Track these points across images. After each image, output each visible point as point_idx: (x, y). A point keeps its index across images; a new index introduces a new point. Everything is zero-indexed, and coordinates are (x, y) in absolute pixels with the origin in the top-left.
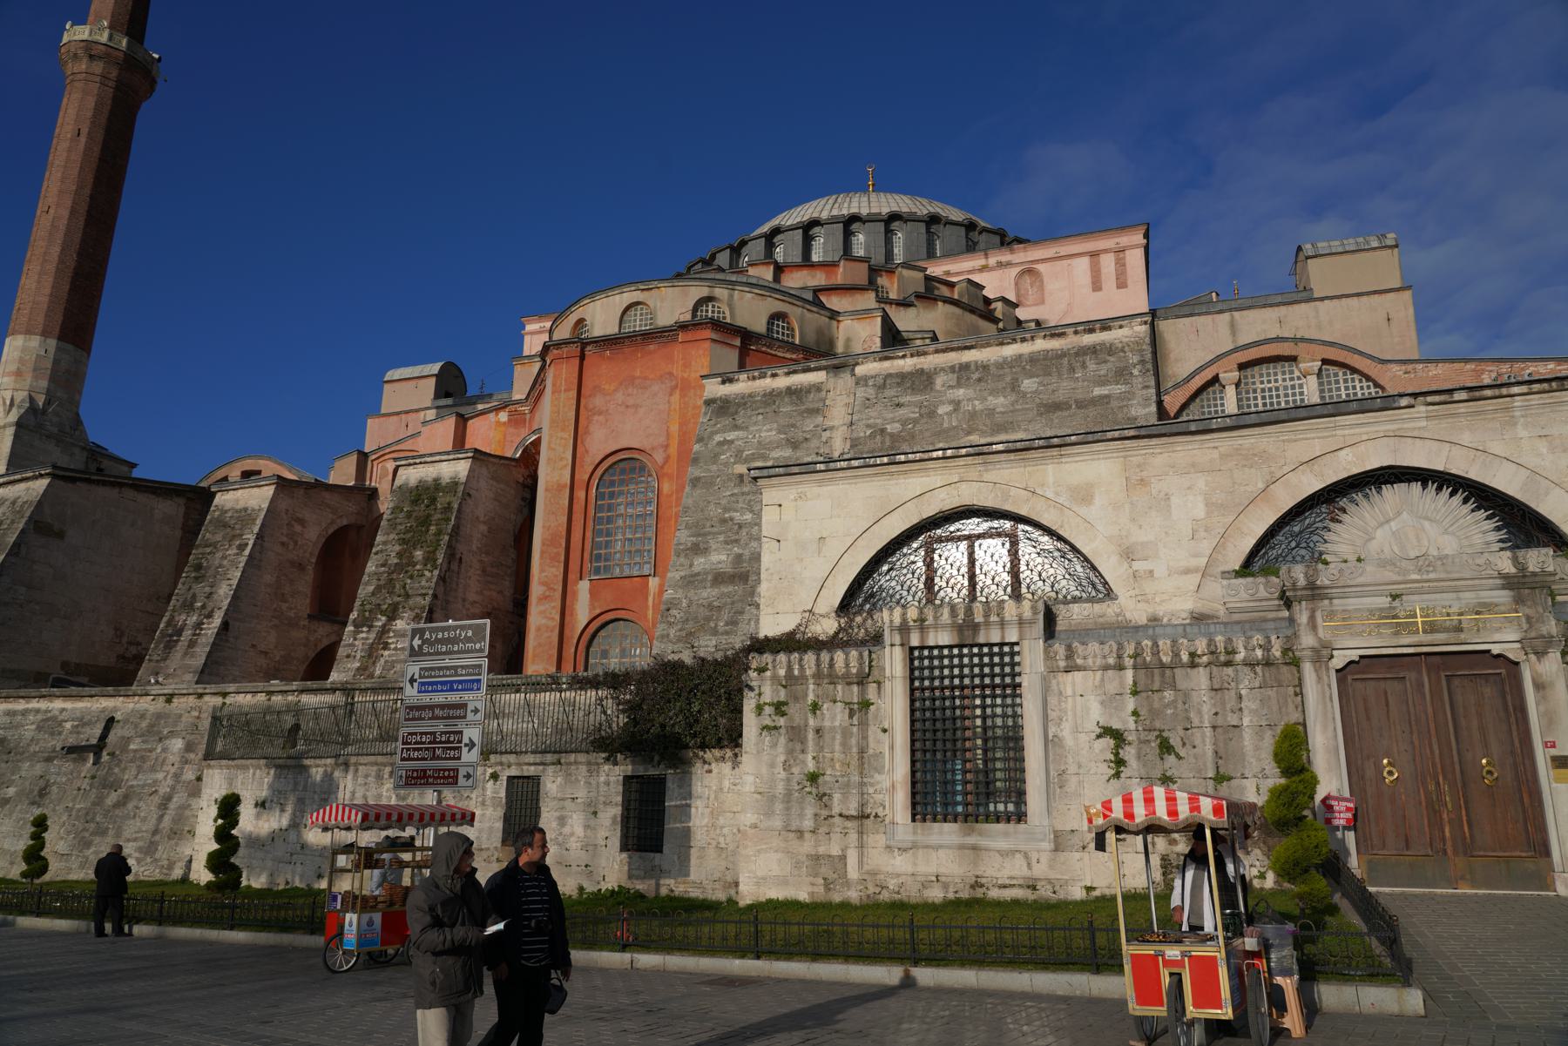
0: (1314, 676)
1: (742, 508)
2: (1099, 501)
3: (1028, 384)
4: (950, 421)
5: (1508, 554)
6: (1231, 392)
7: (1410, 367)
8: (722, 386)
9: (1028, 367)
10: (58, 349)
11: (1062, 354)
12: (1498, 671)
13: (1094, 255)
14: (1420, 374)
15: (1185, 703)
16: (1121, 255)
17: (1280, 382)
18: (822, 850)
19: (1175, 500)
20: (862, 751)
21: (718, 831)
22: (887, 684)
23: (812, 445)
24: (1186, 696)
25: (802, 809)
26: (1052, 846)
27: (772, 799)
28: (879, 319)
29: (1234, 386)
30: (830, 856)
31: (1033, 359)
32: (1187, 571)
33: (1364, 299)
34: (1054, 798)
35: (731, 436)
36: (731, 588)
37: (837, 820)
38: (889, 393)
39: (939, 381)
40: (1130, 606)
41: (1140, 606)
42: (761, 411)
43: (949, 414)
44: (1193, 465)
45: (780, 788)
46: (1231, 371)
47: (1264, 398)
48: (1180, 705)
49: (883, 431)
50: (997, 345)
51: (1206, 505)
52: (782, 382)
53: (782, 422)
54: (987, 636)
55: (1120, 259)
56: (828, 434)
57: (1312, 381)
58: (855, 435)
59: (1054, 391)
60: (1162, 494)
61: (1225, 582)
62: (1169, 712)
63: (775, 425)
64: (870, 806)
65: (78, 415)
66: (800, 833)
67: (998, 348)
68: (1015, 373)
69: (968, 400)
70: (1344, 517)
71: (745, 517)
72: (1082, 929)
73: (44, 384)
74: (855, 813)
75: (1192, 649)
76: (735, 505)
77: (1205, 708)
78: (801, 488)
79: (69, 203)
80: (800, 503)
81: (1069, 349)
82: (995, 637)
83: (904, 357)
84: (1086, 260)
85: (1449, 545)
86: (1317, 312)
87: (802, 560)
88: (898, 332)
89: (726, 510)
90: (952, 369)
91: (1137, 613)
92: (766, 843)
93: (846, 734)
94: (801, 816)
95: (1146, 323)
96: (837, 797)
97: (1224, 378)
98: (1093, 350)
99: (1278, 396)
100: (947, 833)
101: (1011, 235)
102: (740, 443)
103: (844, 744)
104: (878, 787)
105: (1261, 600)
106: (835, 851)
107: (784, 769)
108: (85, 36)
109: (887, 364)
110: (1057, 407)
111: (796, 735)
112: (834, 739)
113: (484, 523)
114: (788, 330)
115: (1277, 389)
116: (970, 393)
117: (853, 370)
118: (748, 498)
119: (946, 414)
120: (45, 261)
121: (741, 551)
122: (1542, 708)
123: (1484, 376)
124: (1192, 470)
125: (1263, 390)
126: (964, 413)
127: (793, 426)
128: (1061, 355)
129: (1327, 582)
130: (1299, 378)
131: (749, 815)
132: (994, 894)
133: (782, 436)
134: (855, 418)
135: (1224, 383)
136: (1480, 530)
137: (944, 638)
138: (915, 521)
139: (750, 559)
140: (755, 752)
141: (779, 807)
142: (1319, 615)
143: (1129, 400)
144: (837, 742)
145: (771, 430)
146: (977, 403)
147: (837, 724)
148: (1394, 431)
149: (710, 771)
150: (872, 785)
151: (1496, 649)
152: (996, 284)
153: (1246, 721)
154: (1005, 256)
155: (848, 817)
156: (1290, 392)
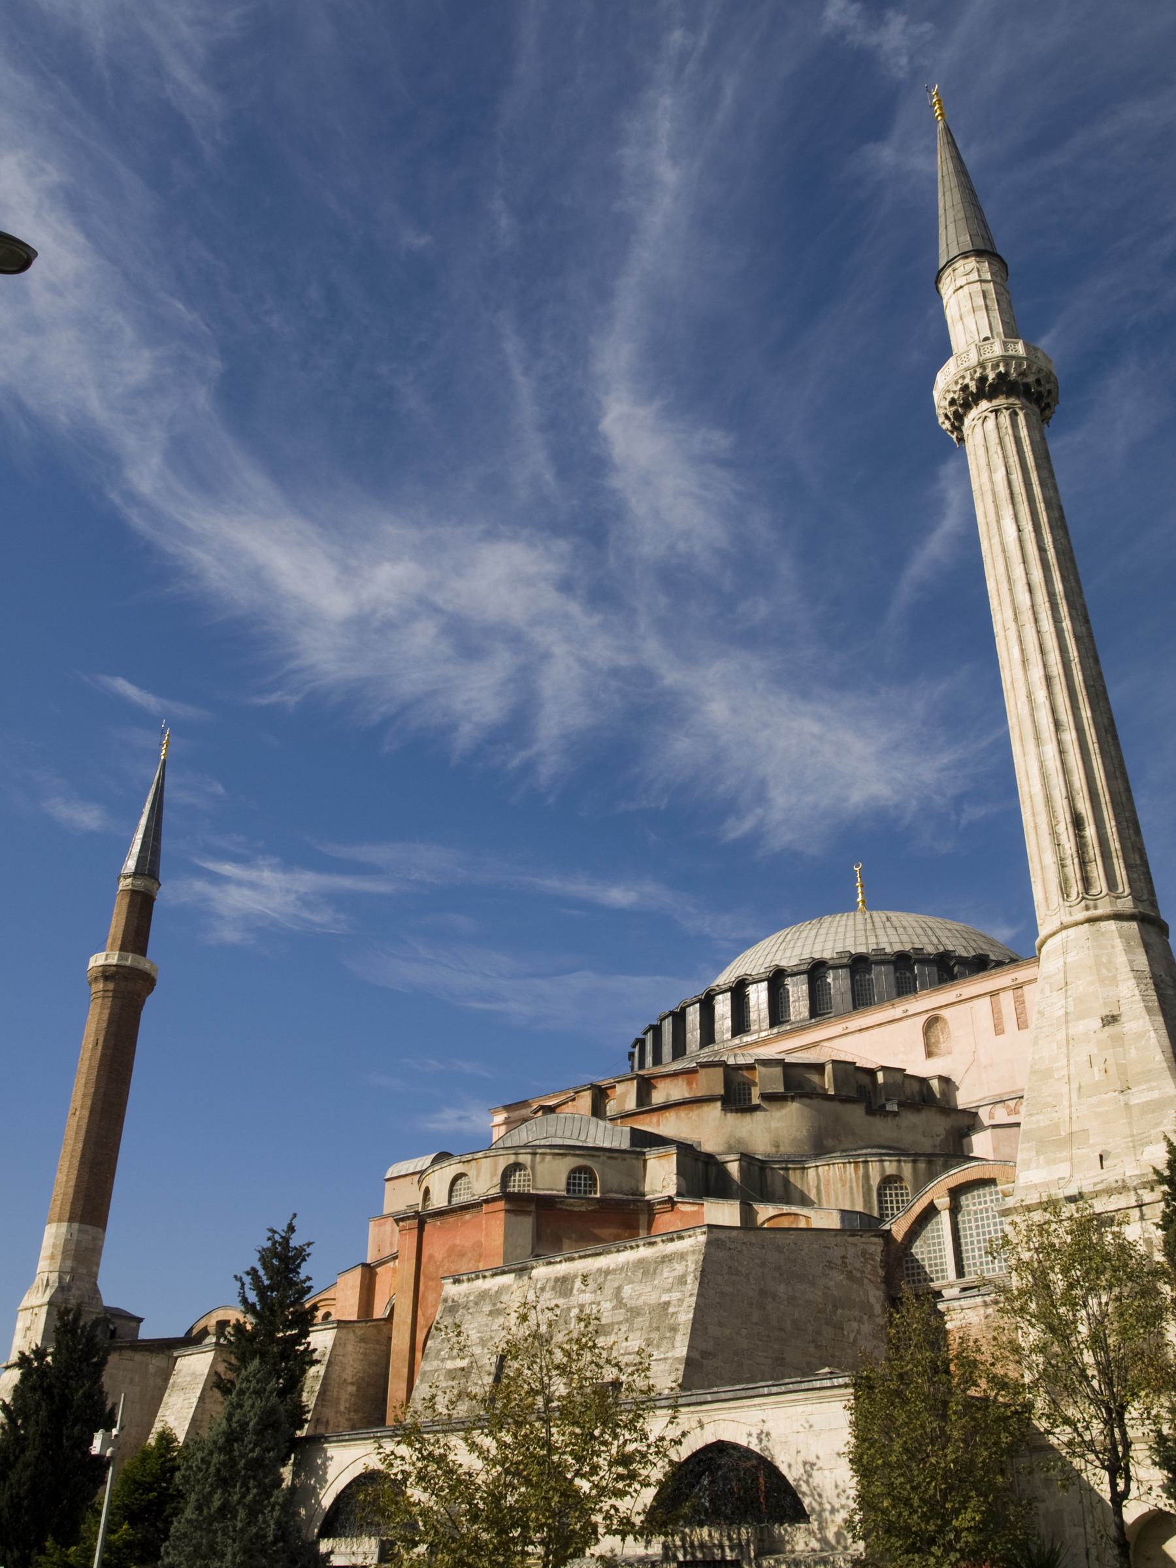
10: (80, 1231)
13: (993, 994)
17: (989, 1204)
28: (675, 1156)
29: (947, 1211)
46: (943, 1197)
47: (976, 1220)
65: (95, 1284)
73: (69, 1263)
79: (89, 1103)
83: (561, 1262)
84: (987, 999)
95: (705, 1233)
108: (101, 962)
109: (550, 1268)
113: (352, 1384)
114: (590, 1180)
115: (987, 1211)
120: (72, 1156)
125: (976, 1213)
146: (594, 1306)
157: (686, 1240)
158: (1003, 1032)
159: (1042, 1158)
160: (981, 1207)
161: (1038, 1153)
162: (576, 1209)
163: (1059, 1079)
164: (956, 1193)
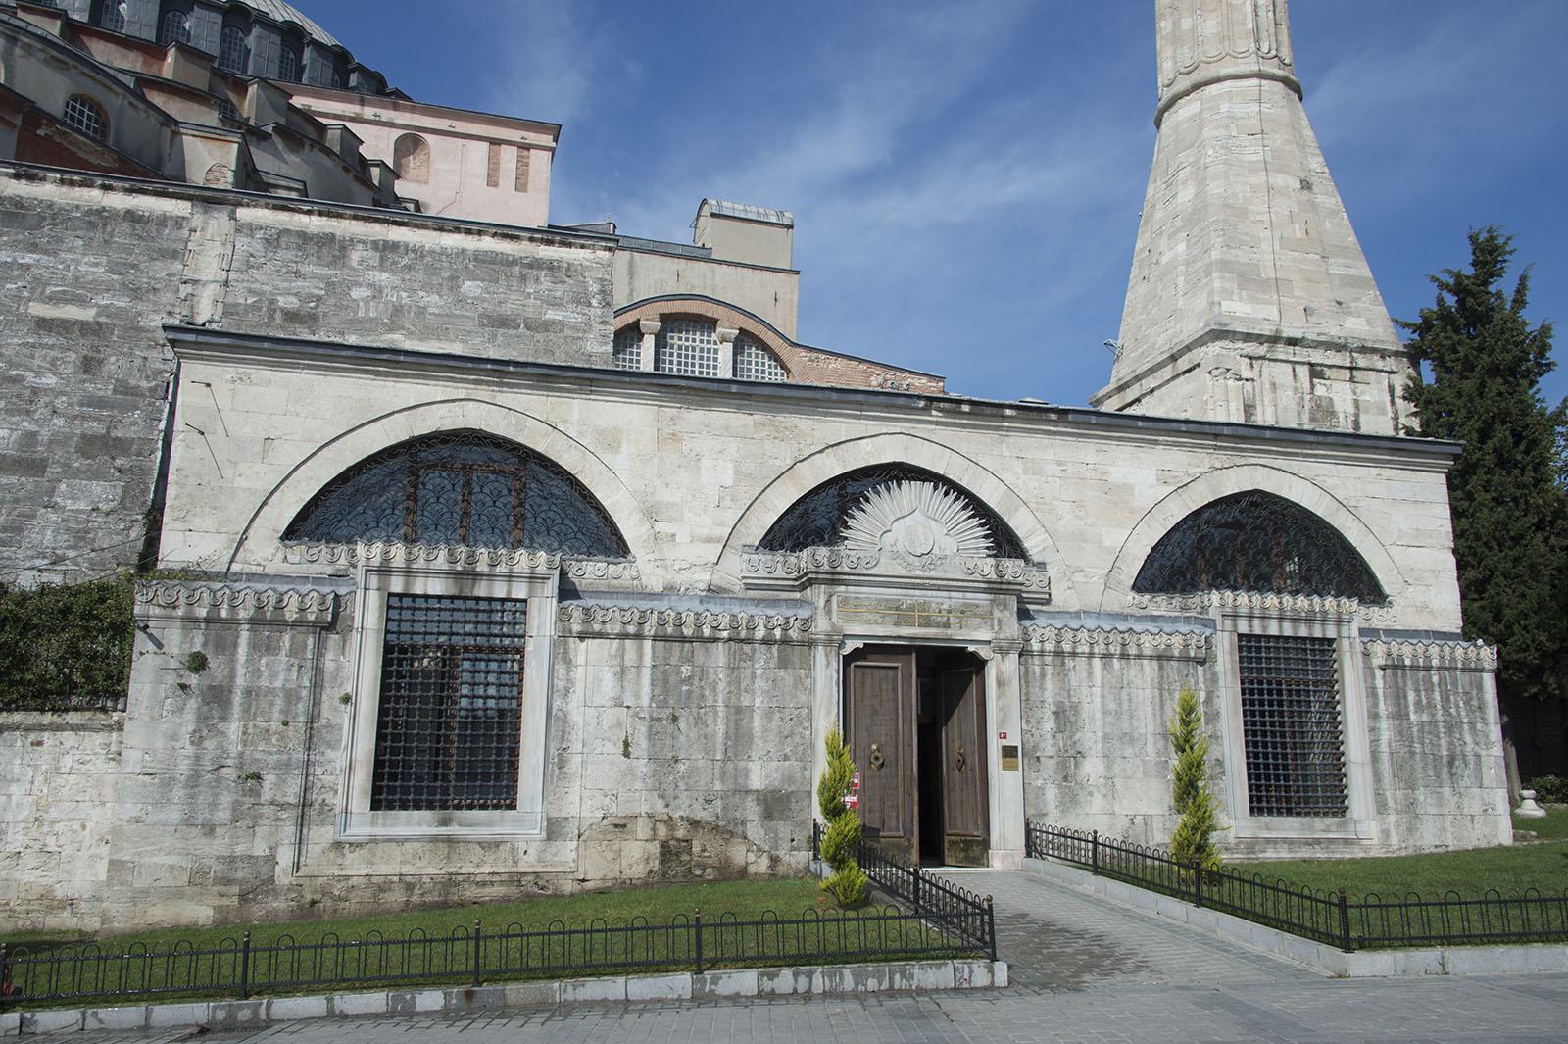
0: (824, 658)
1: (40, 366)
2: (624, 448)
3: (470, 288)
4: (367, 311)
5: (991, 561)
6: (649, 342)
7: (814, 355)
8: (13, 182)
9: (471, 266)
11: (513, 262)
12: (895, 664)
13: (495, 142)
14: (821, 364)
15: (701, 680)
16: (526, 153)
18: (240, 850)
19: (705, 463)
20: (312, 719)
21: (45, 829)
22: (355, 637)
23: (164, 300)
24: (703, 672)
25: (215, 795)
26: (544, 835)
27: (168, 783)
28: (236, 146)
30: (250, 857)
31: (479, 257)
32: (709, 540)
33: (758, 272)
34: (552, 781)
35: (28, 258)
36: (14, 480)
37: (267, 810)
38: (282, 254)
39: (355, 256)
40: (646, 567)
41: (658, 570)
42: (80, 233)
43: (366, 300)
44: (727, 428)
45: (184, 767)
46: (653, 320)
47: (679, 356)
48: (696, 681)
49: (272, 302)
50: (435, 230)
51: (735, 472)
52: (118, 201)
53: (114, 256)
54: (490, 589)
55: (523, 157)
56: (188, 289)
57: (726, 352)
58: (230, 299)
59: (500, 303)
60: (693, 454)
61: (745, 556)
62: (684, 688)
63: (104, 259)
64: (315, 790)
66: (210, 830)
67: (437, 234)
68: (455, 270)
69: (393, 288)
70: (866, 506)
71: (44, 381)
72: (687, 927)
74: (293, 800)
75: (715, 624)
76: (28, 361)
77: (721, 687)
78: (242, 368)
80: (238, 386)
81: (521, 258)
82: (499, 590)
83: (309, 212)
84: (486, 145)
85: (950, 545)
86: (714, 275)
87: (236, 463)
88: (256, 171)
89: (11, 365)
90: (375, 245)
91: (654, 581)
92: (153, 844)
93: (291, 697)
94: (214, 805)
96: (269, 779)
97: (644, 326)
98: (551, 266)
99: (693, 357)
100: (415, 823)
101: (391, 86)
102: (42, 272)
103: (286, 711)
104: (329, 767)
105: (777, 579)
106: (260, 849)
107: (192, 743)
110: (503, 322)
111: (218, 697)
112: (272, 704)
115: (694, 349)
116: (396, 280)
117: (234, 212)
118: (52, 353)
119: (363, 299)
121: (34, 428)
122: (1000, 703)
123: (872, 379)
124: (726, 433)
125: (680, 348)
126: (386, 304)
127: (134, 266)
128: (511, 262)
129: (846, 570)
130: (715, 343)
131: (128, 805)
132: (471, 893)
133: (115, 277)
134: (233, 276)
135: (643, 331)
136: (974, 535)
137: (436, 587)
138: (404, 437)
139: (50, 442)
140: (147, 719)
141: (178, 793)
142: (834, 599)
143: (585, 332)
144: (277, 708)
145: (97, 264)
146: (404, 295)
147: (278, 684)
148: (908, 428)
149: (40, 744)
150: (321, 763)
151: (971, 648)
152: (377, 144)
153: (758, 702)
154: (387, 114)
155: (283, 806)
156: (705, 355)
157: (573, 250)
158: (495, 185)
159: (1244, 293)
160: (687, 344)
161: (1241, 288)
162: (82, 154)
163: (1253, 222)
164: (665, 318)
